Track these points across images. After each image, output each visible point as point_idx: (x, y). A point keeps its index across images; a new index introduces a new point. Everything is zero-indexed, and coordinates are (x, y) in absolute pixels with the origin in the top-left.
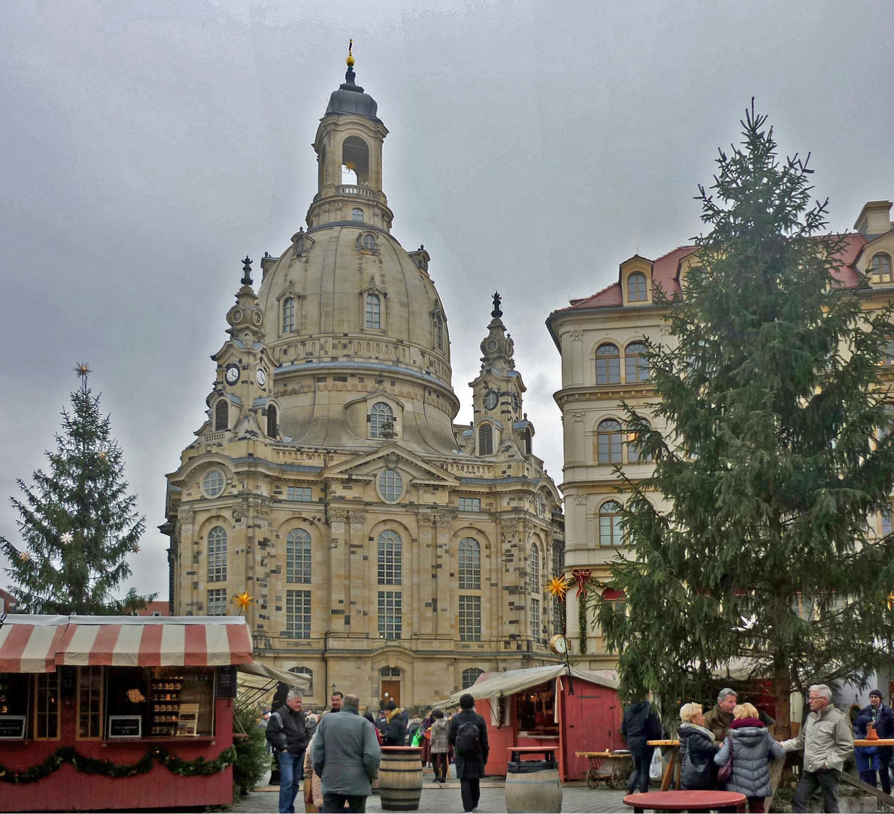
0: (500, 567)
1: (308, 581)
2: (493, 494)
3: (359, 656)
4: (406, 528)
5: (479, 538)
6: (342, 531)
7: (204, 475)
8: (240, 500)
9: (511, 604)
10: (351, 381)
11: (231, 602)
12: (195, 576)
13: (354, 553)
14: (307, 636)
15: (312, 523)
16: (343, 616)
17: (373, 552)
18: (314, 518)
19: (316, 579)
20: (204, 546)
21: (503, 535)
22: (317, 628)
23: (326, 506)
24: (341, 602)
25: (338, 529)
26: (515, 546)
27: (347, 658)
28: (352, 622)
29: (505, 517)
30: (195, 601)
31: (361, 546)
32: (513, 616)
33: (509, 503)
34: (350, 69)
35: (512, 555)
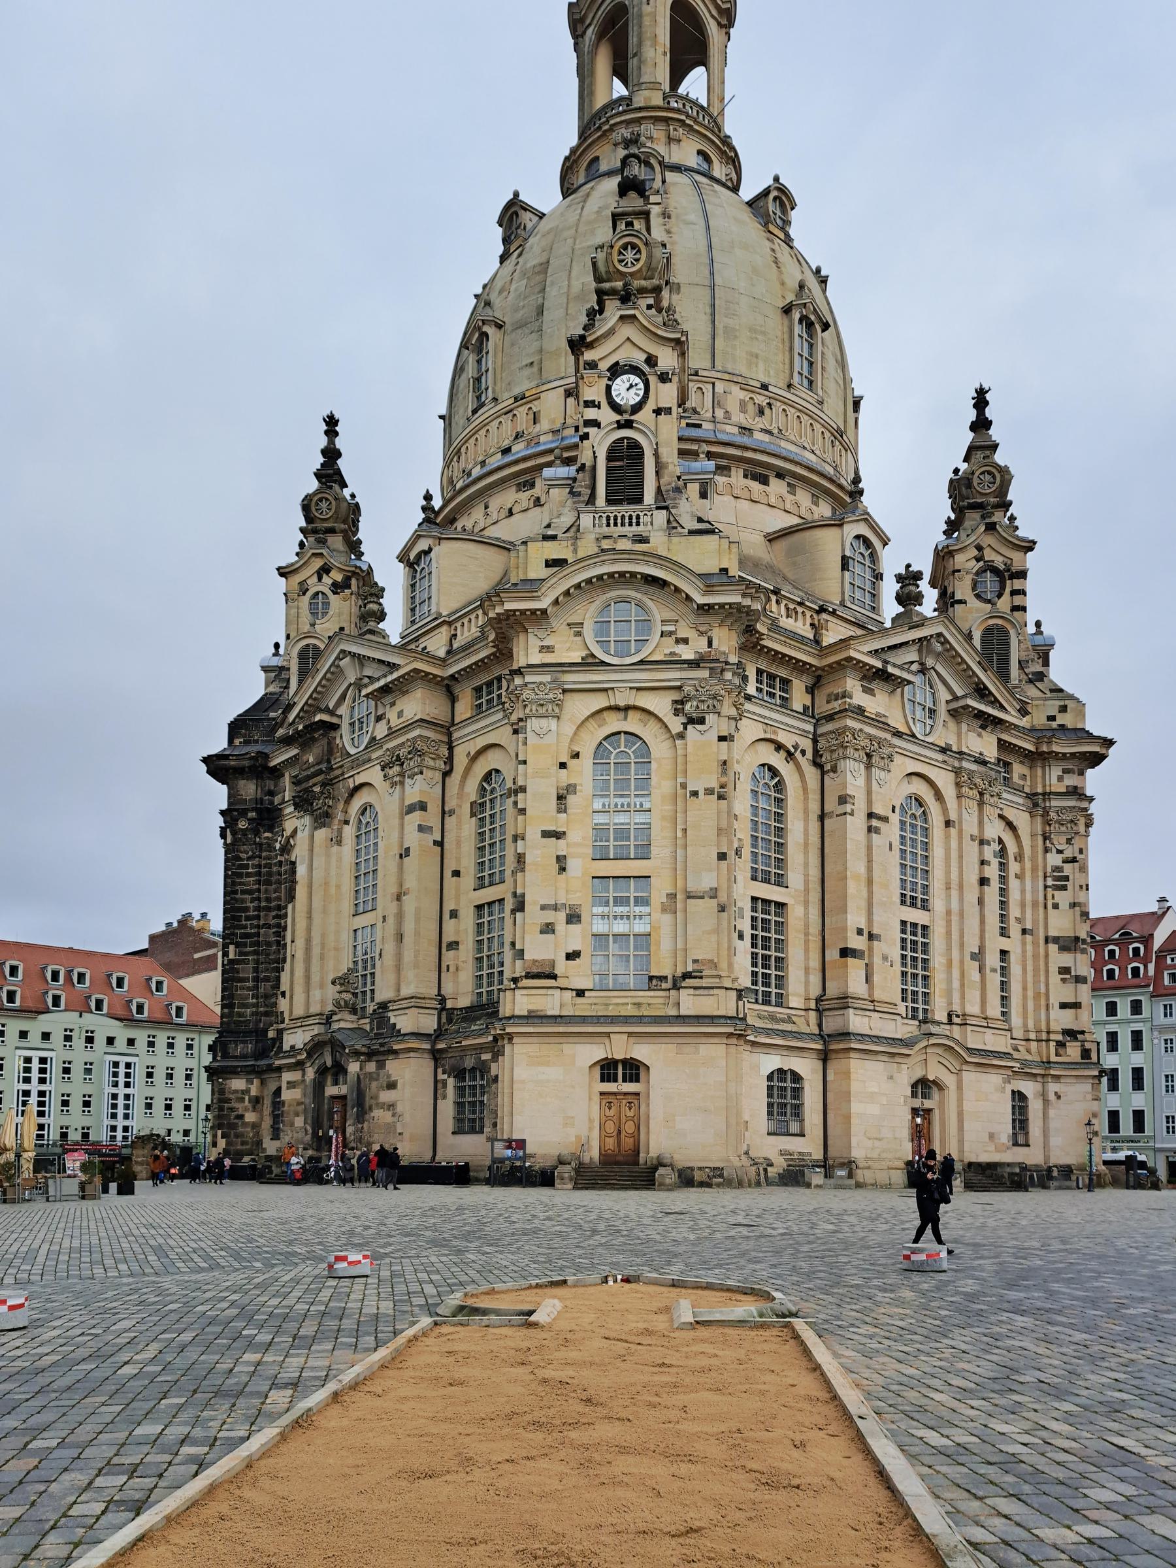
1: (780, 881)
4: (939, 796)
5: (1008, 839)
6: (861, 781)
7: (594, 608)
8: (705, 674)
9: (1065, 970)
11: (664, 910)
12: (560, 841)
13: (877, 831)
15: (790, 755)
17: (891, 831)
18: (796, 747)
19: (794, 877)
20: (583, 773)
21: (1046, 838)
23: (816, 726)
25: (853, 776)
26: (1074, 860)
29: (1056, 803)
30: (562, 901)
31: (885, 819)
32: (1066, 993)
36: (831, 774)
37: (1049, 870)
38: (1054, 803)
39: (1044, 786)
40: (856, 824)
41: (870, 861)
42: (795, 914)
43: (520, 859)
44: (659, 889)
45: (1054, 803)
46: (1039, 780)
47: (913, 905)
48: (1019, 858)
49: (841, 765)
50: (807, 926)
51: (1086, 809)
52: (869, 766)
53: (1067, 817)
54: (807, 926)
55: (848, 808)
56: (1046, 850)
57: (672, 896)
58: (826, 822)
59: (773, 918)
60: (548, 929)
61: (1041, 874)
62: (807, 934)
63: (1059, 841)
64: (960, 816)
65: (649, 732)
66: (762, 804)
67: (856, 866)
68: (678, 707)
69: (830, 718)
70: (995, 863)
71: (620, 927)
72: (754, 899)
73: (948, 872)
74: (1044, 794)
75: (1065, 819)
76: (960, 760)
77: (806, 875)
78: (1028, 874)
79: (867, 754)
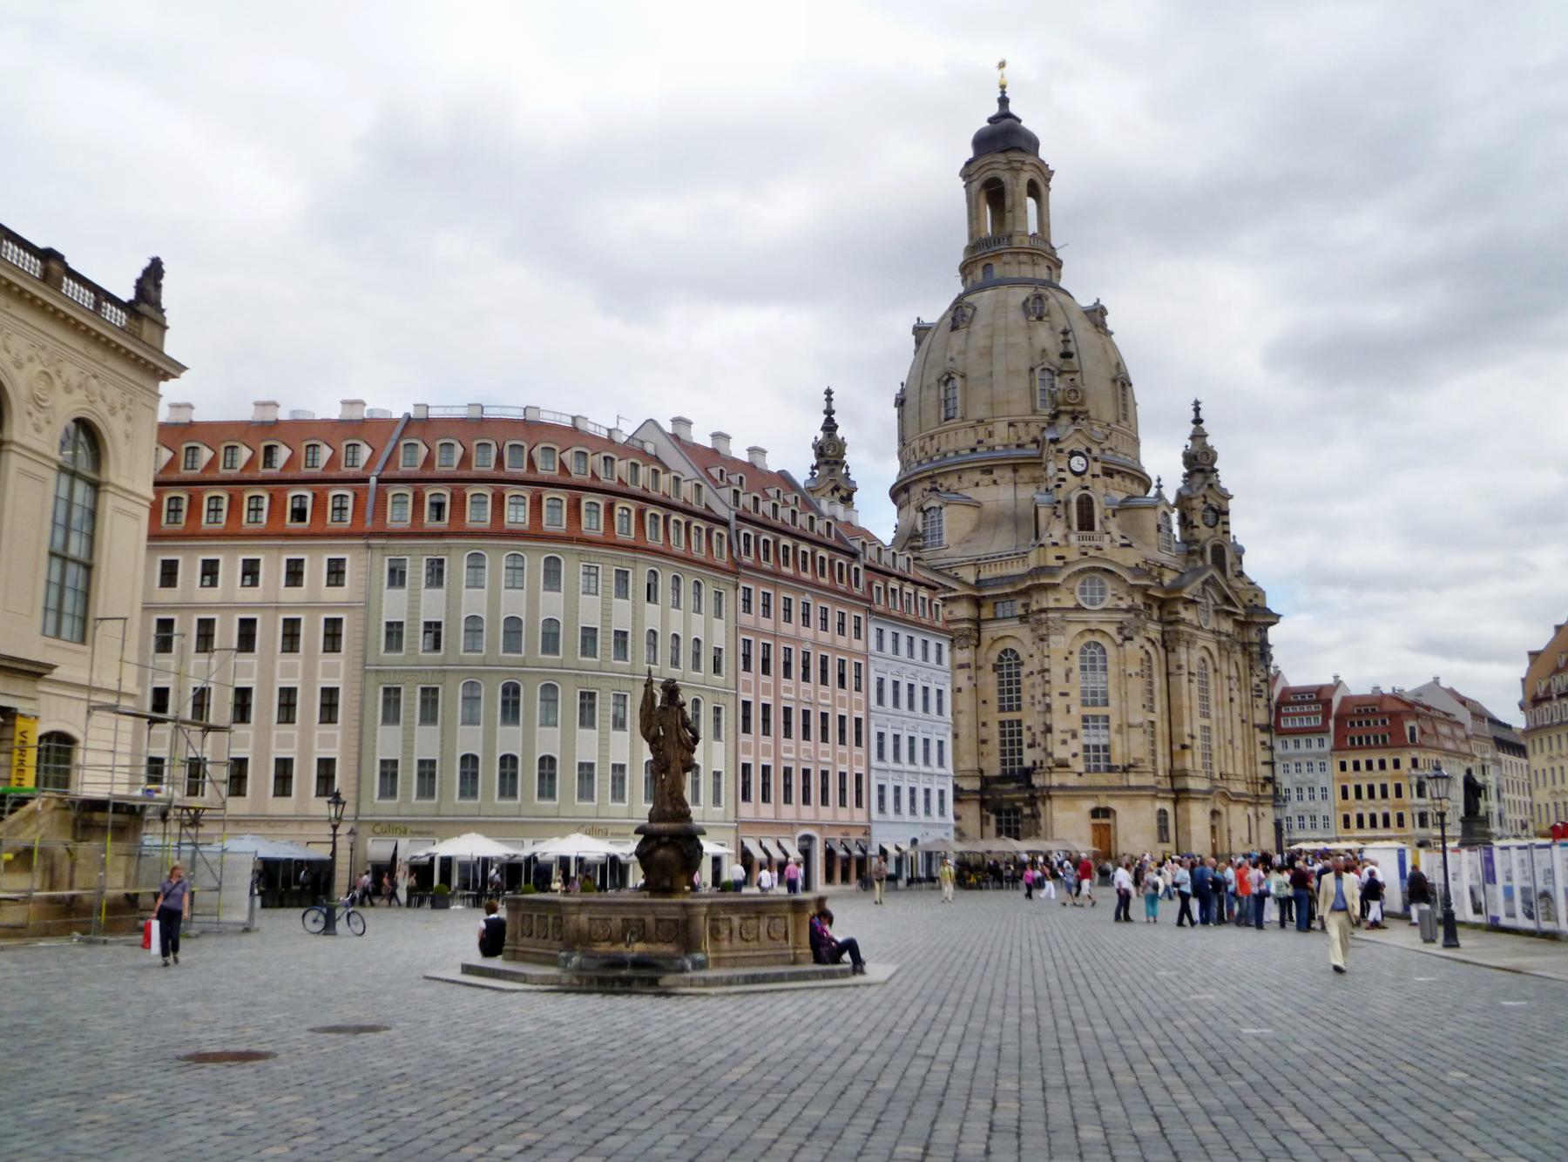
1: (1152, 710)
10: (1117, 479)
15: (1153, 643)
19: (1157, 708)
20: (1076, 661)
21: (1251, 668)
25: (1182, 654)
34: (1003, 92)
40: (1185, 679)
42: (1158, 725)
43: (1048, 707)
44: (1114, 724)
57: (1120, 726)
60: (1064, 742)
63: (1257, 671)
65: (1105, 642)
68: (1120, 631)
69: (1170, 623)
71: (1094, 741)
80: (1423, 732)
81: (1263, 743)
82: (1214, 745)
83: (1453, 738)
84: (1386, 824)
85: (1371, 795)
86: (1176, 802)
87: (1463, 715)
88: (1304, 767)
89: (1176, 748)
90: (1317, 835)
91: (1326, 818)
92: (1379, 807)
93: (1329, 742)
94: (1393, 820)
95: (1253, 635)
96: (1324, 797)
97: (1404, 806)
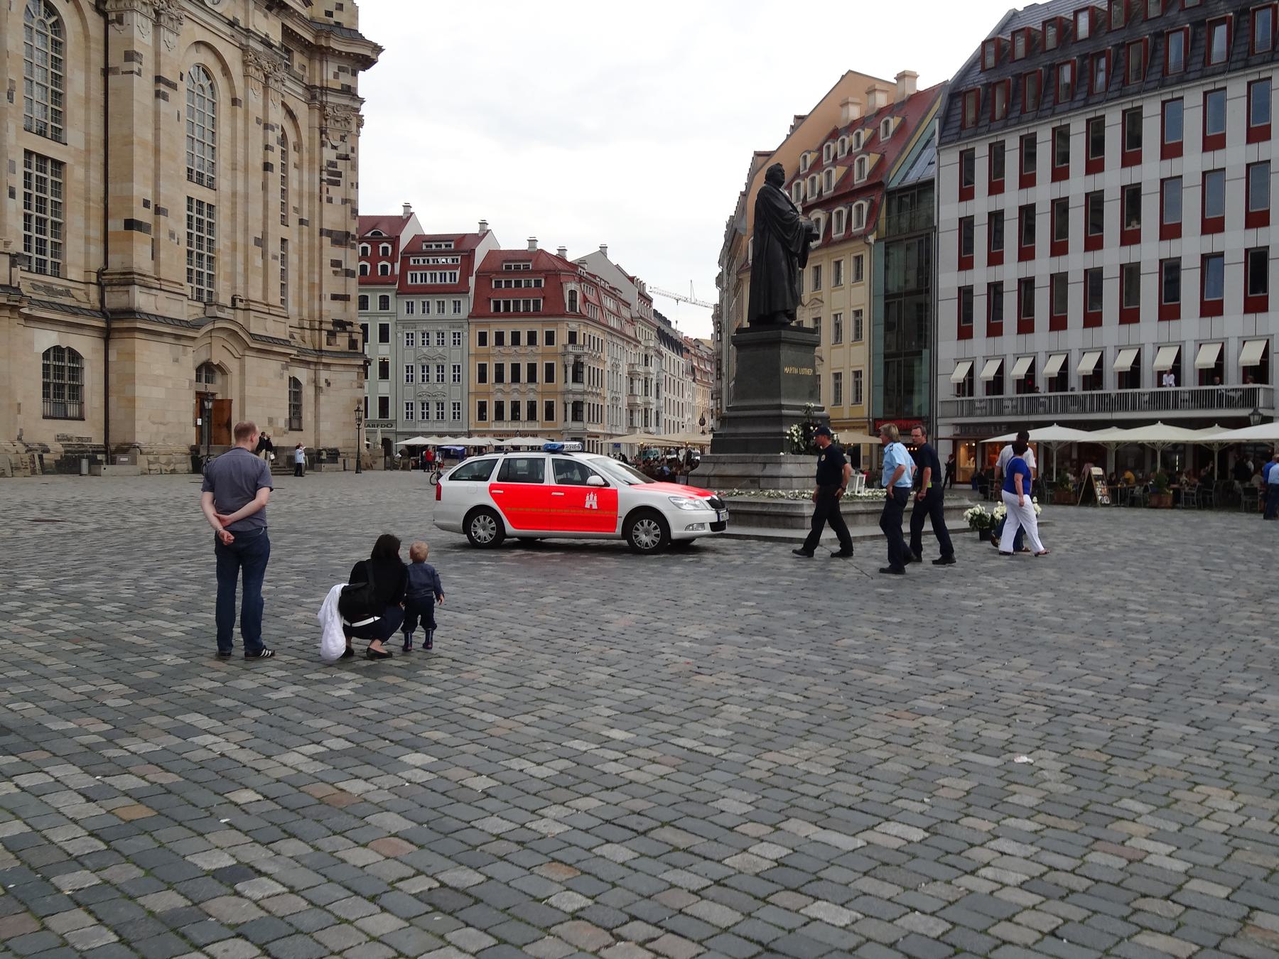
0: (317, 191)
1: (58, 136)
2: (317, 52)
3: (180, 331)
4: (226, 71)
6: (149, 39)
13: (165, 97)
14: (57, 271)
16: (148, 238)
19: (74, 134)
22: (80, 255)
24: (146, 204)
25: (140, 31)
26: (346, 158)
27: (161, 334)
28: (163, 255)
29: (331, 99)
31: (173, 86)
33: (336, 76)
35: (340, 174)
36: (117, 25)
37: (325, 164)
38: (330, 99)
39: (322, 80)
40: (143, 87)
41: (157, 129)
45: (330, 99)
46: (317, 74)
47: (200, 182)
48: (298, 147)
49: (127, 17)
50: (87, 190)
51: (358, 110)
52: (157, 25)
53: (341, 114)
54: (87, 190)
55: (135, 67)
56: (323, 144)
58: (111, 77)
59: (49, 177)
61: (317, 167)
62: (88, 200)
64: (246, 97)
66: (38, 42)
67: (143, 132)
70: (278, 148)
72: (28, 153)
73: (234, 153)
74: (322, 88)
75: (338, 116)
76: (247, 37)
77: (87, 134)
78: (306, 165)
79: (156, 11)
80: (585, 300)
81: (336, 263)
82: (222, 243)
83: (617, 315)
84: (532, 416)
85: (516, 378)
86: (107, 336)
87: (630, 294)
88: (434, 339)
89: (116, 225)
90: (444, 428)
91: (457, 406)
92: (524, 393)
93: (467, 305)
94: (541, 411)
95: (329, 73)
96: (457, 378)
97: (555, 393)
